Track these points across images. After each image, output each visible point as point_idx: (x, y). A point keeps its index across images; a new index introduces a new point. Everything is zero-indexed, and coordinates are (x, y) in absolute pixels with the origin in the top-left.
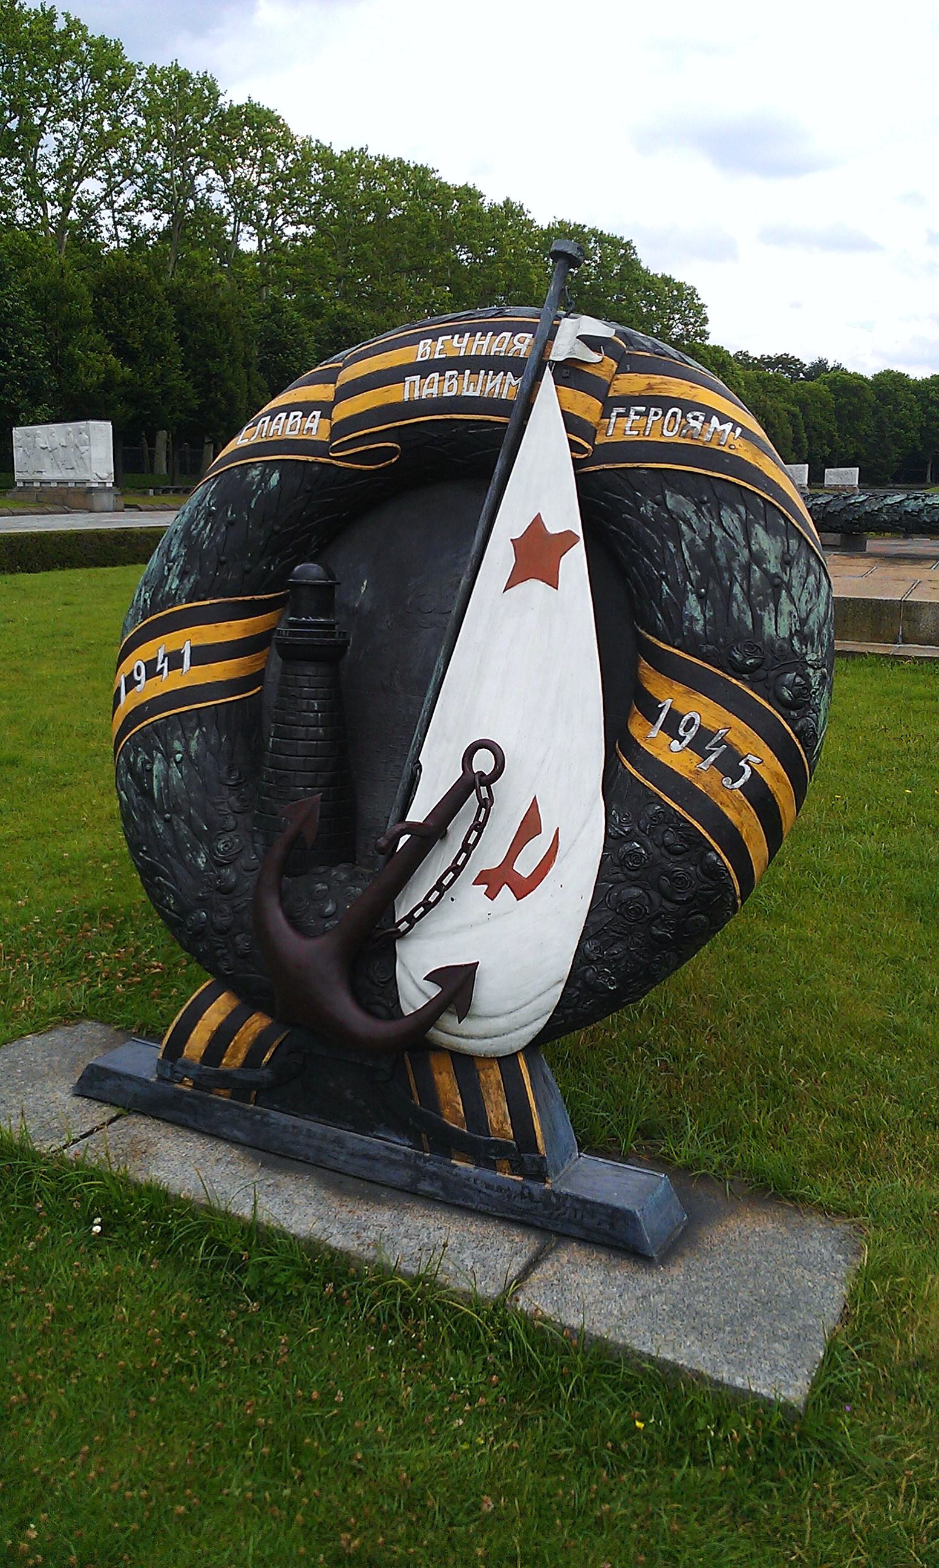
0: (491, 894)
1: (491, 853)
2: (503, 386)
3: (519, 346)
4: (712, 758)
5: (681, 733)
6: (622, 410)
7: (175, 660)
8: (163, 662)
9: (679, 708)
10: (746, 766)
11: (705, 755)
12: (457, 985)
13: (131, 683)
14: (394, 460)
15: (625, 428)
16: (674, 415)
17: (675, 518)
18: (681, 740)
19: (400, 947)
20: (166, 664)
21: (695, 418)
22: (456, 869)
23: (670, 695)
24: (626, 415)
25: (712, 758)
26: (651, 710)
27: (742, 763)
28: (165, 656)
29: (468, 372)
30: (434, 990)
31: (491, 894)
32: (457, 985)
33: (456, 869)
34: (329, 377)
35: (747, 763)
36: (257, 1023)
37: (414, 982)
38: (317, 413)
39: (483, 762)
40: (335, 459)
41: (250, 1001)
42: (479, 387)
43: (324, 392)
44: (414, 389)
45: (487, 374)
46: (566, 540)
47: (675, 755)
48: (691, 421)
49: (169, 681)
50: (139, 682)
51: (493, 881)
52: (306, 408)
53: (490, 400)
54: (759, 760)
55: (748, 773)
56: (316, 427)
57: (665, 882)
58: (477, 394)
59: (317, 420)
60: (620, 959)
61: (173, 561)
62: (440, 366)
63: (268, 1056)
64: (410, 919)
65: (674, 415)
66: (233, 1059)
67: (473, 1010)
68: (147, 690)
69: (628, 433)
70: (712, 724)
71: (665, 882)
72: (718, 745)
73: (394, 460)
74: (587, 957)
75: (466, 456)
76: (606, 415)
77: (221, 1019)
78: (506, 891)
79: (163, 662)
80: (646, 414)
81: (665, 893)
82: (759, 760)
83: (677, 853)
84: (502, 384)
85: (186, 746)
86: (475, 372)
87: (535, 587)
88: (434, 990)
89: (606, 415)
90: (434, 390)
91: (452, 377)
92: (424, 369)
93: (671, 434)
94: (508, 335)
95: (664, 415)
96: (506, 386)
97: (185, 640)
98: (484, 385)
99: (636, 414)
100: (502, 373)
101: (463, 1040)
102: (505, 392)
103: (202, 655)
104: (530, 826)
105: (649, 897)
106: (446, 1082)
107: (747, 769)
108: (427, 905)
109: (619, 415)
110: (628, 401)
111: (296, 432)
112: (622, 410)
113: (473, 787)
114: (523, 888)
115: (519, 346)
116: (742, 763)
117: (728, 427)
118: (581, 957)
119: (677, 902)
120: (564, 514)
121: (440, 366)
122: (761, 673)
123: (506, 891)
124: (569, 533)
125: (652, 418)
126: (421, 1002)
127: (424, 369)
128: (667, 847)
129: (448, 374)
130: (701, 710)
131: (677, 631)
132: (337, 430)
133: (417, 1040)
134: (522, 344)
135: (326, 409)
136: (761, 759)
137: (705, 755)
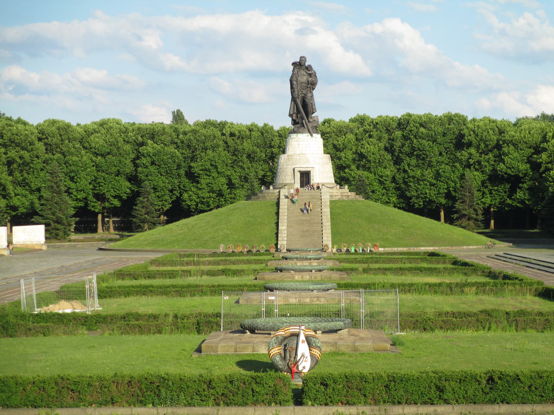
2: (298, 330)
12: (304, 367)
15: (307, 333)
23: (313, 350)
32: (304, 367)
44: (291, 330)
47: (314, 353)
56: (283, 333)
68: (274, 353)
75: (297, 335)
81: (315, 362)
113: (303, 355)
130: (315, 350)
133: (301, 372)
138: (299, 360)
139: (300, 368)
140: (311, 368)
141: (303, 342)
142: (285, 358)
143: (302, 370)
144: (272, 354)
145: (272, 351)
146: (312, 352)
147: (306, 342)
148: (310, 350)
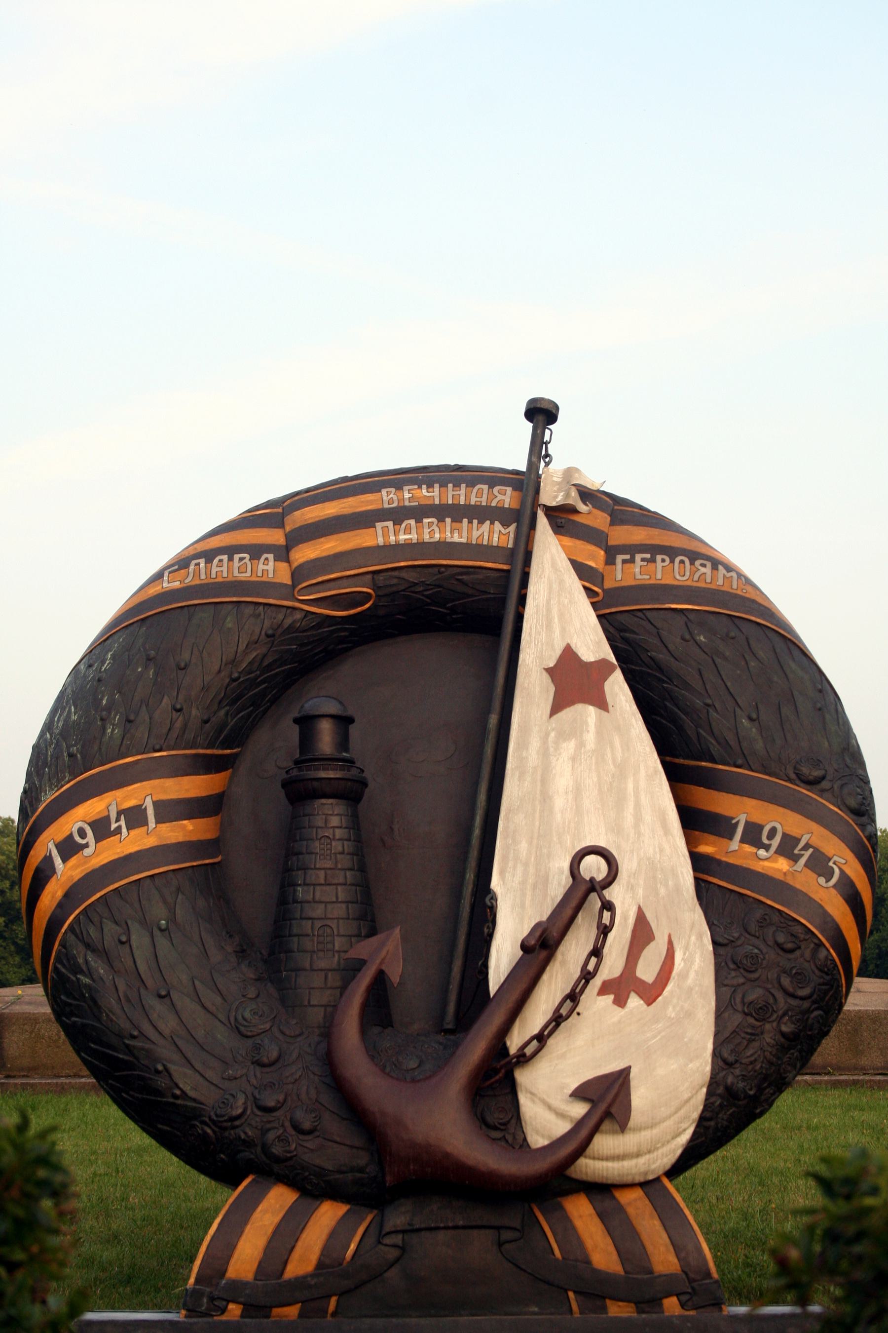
0: (621, 1002)
1: (613, 964)
3: (500, 497)
4: (803, 861)
5: (765, 840)
6: (628, 557)
8: (118, 820)
9: (757, 818)
10: (834, 866)
11: (795, 859)
12: (607, 1099)
14: (367, 606)
16: (682, 562)
18: (767, 848)
19: (522, 1077)
20: (122, 823)
21: (704, 566)
22: (587, 976)
23: (742, 810)
24: (632, 561)
25: (803, 861)
26: (721, 826)
27: (831, 864)
28: (119, 814)
29: (448, 520)
30: (579, 1109)
31: (621, 1002)
32: (607, 1099)
33: (587, 976)
35: (834, 863)
36: (328, 1215)
37: (550, 1107)
38: (271, 556)
41: (313, 1187)
42: (465, 534)
44: (384, 534)
45: (470, 522)
46: (601, 669)
48: (700, 568)
49: (129, 842)
50: (86, 846)
51: (620, 989)
52: (256, 552)
53: (479, 546)
54: (844, 861)
55: (837, 871)
56: (270, 569)
57: (786, 981)
58: (464, 540)
59: (271, 563)
60: (755, 1060)
61: (109, 708)
62: (419, 512)
63: (353, 1247)
64: (541, 1038)
65: (682, 562)
66: (304, 1259)
67: (631, 1124)
68: (96, 855)
69: (639, 577)
70: (794, 832)
71: (786, 981)
72: (807, 847)
73: (367, 606)
74: (725, 1061)
76: (610, 561)
77: (277, 1219)
78: (634, 1001)
79: (118, 820)
80: (653, 560)
82: (844, 861)
83: (791, 951)
84: (491, 532)
85: (172, 911)
86: (457, 520)
88: (579, 1109)
89: (610, 561)
90: (413, 537)
91: (430, 525)
92: (398, 515)
93: (684, 578)
94: (485, 487)
95: (672, 561)
96: (496, 536)
97: (144, 794)
98: (470, 531)
99: (643, 560)
100: (488, 522)
101: (610, 1164)
102: (496, 539)
103: (168, 811)
104: (642, 932)
105: (773, 995)
107: (837, 871)
108: (557, 1020)
109: (624, 562)
110: (632, 550)
111: (248, 574)
112: (628, 557)
113: (585, 894)
114: (651, 993)
115: (500, 497)
116: (831, 864)
117: (733, 574)
119: (802, 998)
121: (419, 512)
122: (825, 784)
123: (634, 1001)
124: (603, 662)
125: (659, 564)
126: (562, 1128)
127: (398, 515)
128: (779, 945)
129: (426, 521)
130: (780, 820)
132: (297, 574)
133: (558, 1179)
135: (283, 553)
137: (795, 859)
139: (547, 1103)
142: (271, 952)
143: (580, 1140)
144: (66, 873)
145: (74, 821)
146: (734, 850)
148: (693, 821)
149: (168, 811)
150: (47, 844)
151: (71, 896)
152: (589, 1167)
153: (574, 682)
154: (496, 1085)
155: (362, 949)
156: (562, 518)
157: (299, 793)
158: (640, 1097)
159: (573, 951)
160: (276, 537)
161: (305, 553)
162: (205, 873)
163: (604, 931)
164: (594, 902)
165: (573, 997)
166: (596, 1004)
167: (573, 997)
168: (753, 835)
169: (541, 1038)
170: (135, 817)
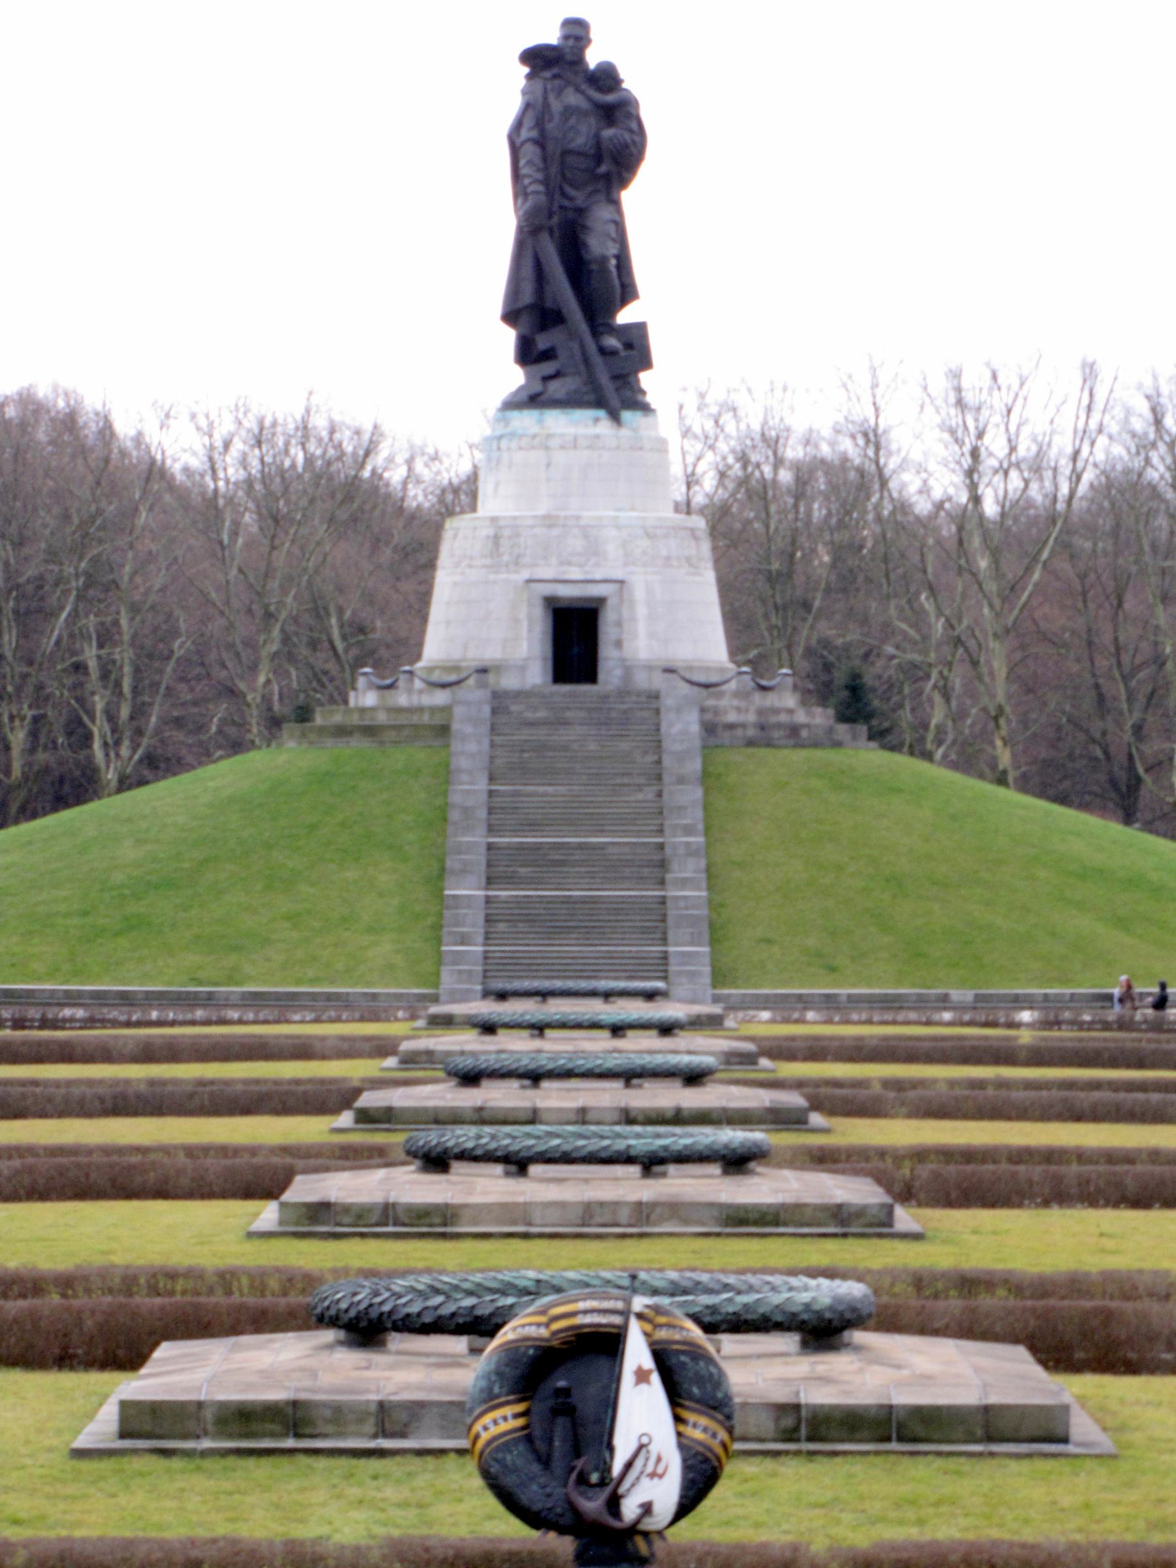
2: (617, 1320)
7: (495, 1422)
12: (647, 1509)
13: (486, 1428)
15: (662, 1334)
17: (684, 1364)
32: (647, 1509)
34: (543, 1312)
39: (645, 1440)
40: (555, 1343)
43: (543, 1319)
46: (650, 1372)
47: (698, 1434)
49: (504, 1427)
51: (653, 1475)
52: (539, 1325)
56: (544, 1332)
68: (494, 1431)
78: (656, 1480)
87: (643, 1386)
92: (585, 1312)
97: (508, 1411)
103: (517, 1416)
104: (659, 1460)
106: (640, 1542)
108: (633, 1485)
110: (661, 1326)
114: (661, 1476)
118: (682, 1497)
120: (648, 1363)
130: (703, 1421)
131: (691, 1397)
133: (633, 1530)
134: (620, 1305)
135: (547, 1325)
136: (723, 1435)
138: (629, 1465)
139: (630, 1509)
140: (685, 1508)
141: (642, 1376)
143: (638, 1521)
144: (485, 1436)
146: (688, 1431)
147: (655, 1378)
148: (678, 1419)
149: (517, 1416)
150: (478, 1427)
151: (489, 1443)
152: (642, 1527)
153: (642, 1376)
154: (614, 1504)
155: (575, 1463)
156: (640, 1316)
157: (555, 1412)
158: (656, 1508)
159: (638, 1464)
160: (543, 1319)
161: (556, 1326)
162: (527, 1437)
163: (647, 1459)
164: (644, 1451)
165: (638, 1479)
166: (645, 1482)
167: (638, 1479)
168: (695, 1425)
169: (629, 1490)
170: (505, 1418)
